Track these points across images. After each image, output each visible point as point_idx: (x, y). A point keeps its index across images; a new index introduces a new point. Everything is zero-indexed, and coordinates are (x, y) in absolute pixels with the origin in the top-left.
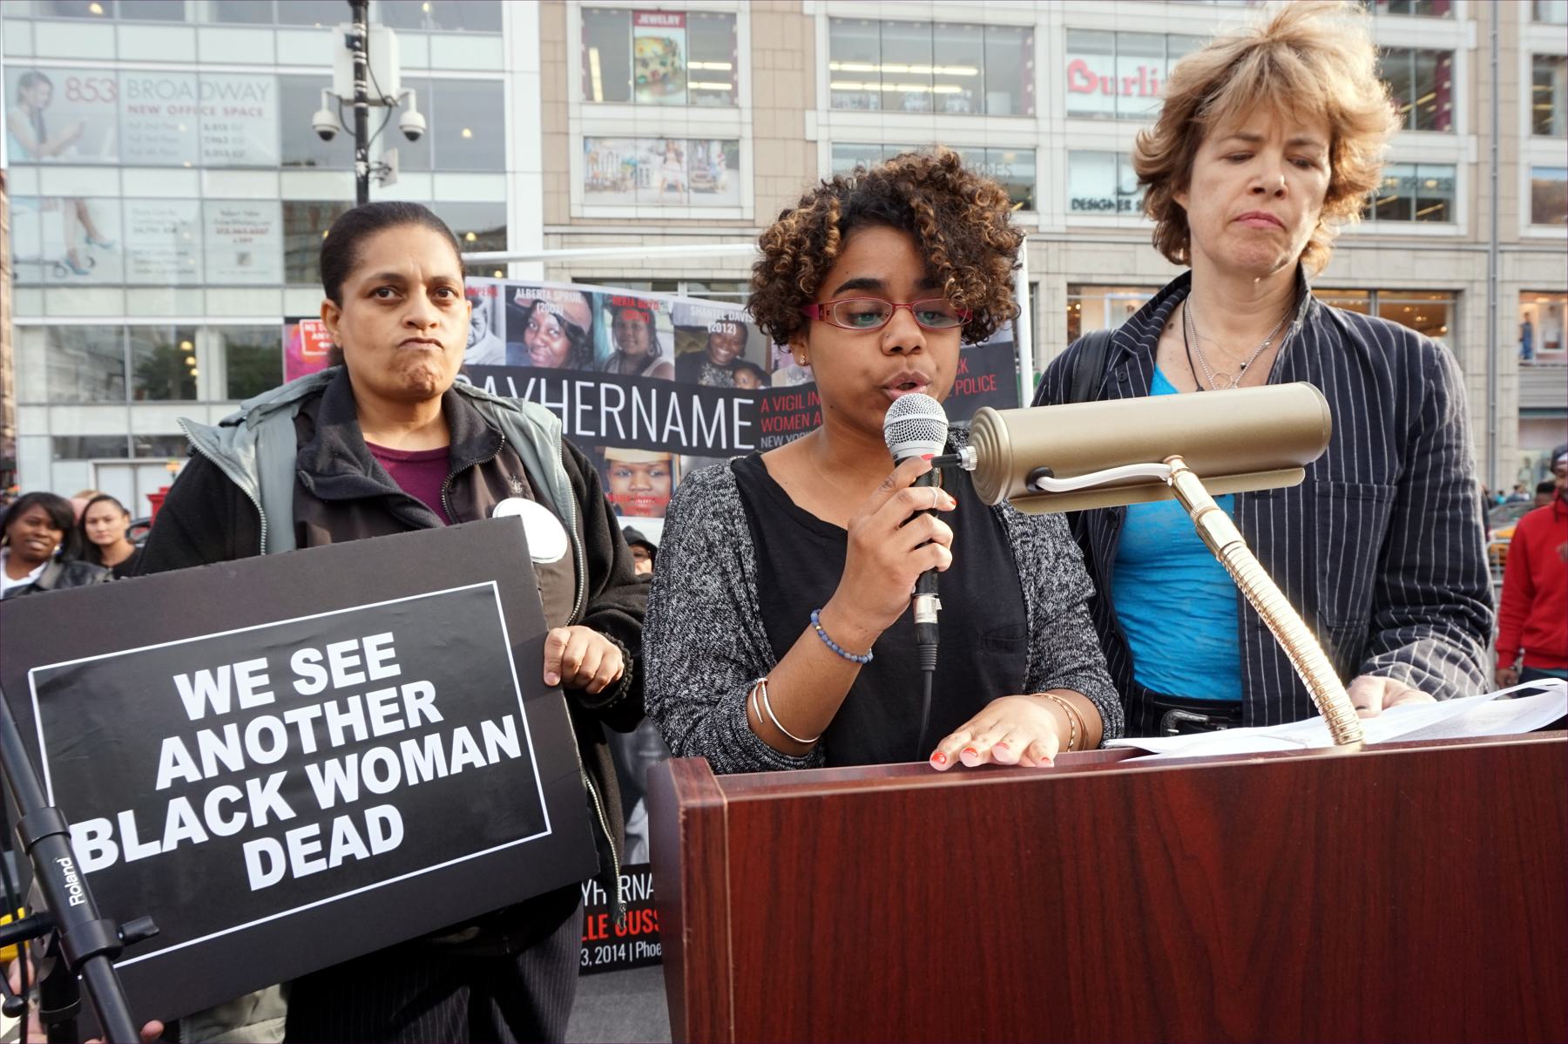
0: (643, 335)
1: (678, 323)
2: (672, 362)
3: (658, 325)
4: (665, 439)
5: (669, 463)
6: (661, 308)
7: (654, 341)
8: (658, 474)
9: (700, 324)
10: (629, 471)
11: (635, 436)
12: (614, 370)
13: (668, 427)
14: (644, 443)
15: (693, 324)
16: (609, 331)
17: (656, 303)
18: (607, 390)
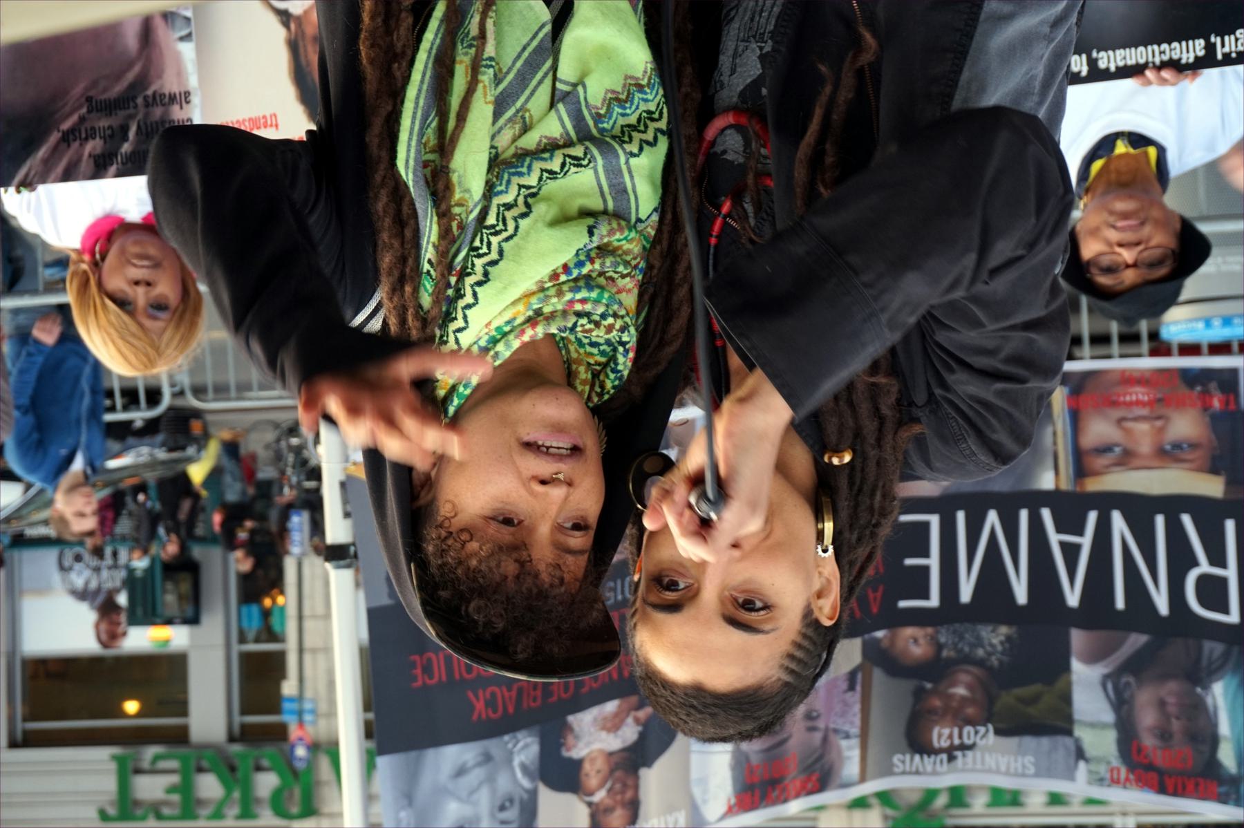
0: (1147, 718)
1: (1068, 741)
2: (1078, 667)
3: (1111, 736)
4: (1092, 517)
5: (1081, 471)
6: (1103, 770)
7: (1122, 705)
8: (1105, 449)
9: (1013, 742)
10: (1168, 454)
11: (1160, 520)
12: (1212, 648)
13: (1086, 541)
14: (1139, 509)
15: (1029, 741)
16: (1224, 728)
17: (1115, 782)
18: (1226, 611)
